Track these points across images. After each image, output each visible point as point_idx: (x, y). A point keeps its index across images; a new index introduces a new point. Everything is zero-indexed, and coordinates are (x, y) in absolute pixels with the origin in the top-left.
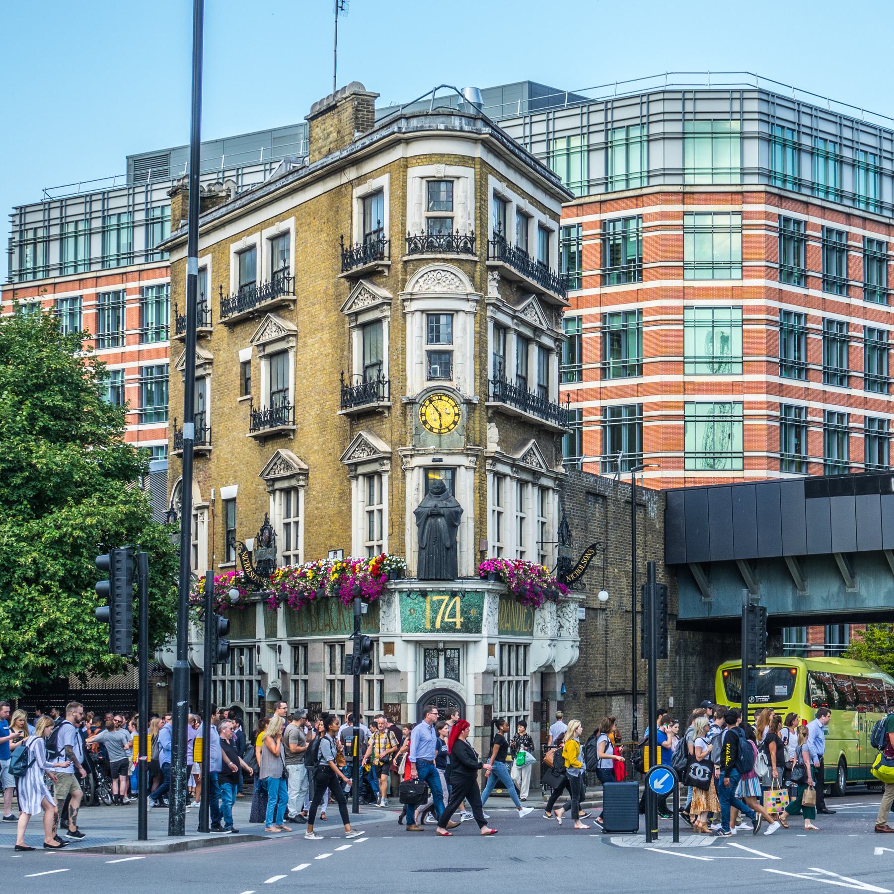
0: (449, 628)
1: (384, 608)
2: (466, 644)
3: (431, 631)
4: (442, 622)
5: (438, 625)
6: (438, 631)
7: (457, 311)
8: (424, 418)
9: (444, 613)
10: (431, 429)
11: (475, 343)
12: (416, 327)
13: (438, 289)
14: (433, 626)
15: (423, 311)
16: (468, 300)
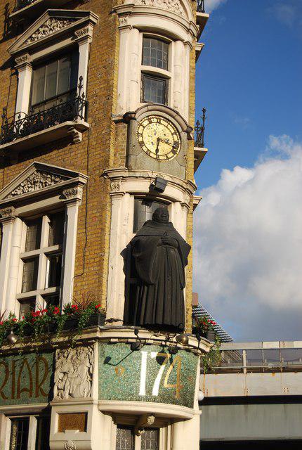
0: (165, 397)
1: (67, 366)
2: (170, 421)
3: (147, 399)
4: (160, 387)
5: (155, 392)
6: (155, 400)
7: (176, 38)
8: (140, 139)
9: (164, 376)
10: (148, 153)
11: (191, 77)
12: (130, 47)
13: (165, 7)
14: (149, 390)
15: (141, 29)
16: (188, 30)
